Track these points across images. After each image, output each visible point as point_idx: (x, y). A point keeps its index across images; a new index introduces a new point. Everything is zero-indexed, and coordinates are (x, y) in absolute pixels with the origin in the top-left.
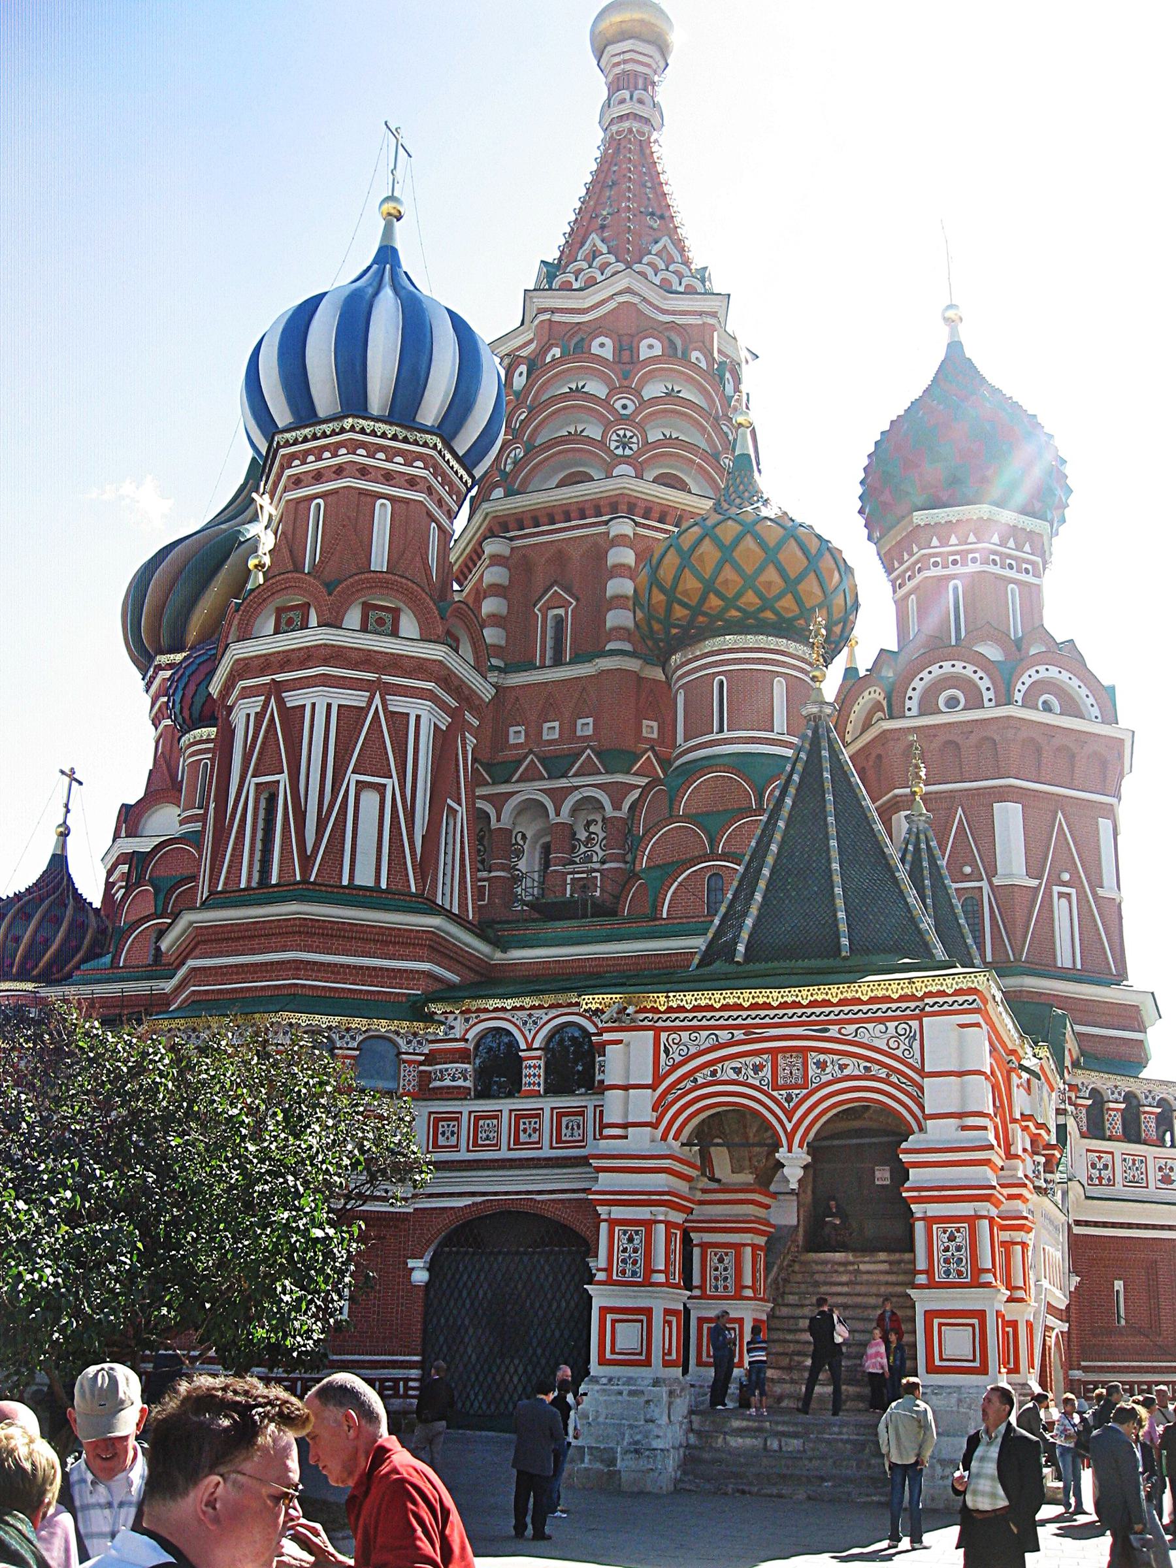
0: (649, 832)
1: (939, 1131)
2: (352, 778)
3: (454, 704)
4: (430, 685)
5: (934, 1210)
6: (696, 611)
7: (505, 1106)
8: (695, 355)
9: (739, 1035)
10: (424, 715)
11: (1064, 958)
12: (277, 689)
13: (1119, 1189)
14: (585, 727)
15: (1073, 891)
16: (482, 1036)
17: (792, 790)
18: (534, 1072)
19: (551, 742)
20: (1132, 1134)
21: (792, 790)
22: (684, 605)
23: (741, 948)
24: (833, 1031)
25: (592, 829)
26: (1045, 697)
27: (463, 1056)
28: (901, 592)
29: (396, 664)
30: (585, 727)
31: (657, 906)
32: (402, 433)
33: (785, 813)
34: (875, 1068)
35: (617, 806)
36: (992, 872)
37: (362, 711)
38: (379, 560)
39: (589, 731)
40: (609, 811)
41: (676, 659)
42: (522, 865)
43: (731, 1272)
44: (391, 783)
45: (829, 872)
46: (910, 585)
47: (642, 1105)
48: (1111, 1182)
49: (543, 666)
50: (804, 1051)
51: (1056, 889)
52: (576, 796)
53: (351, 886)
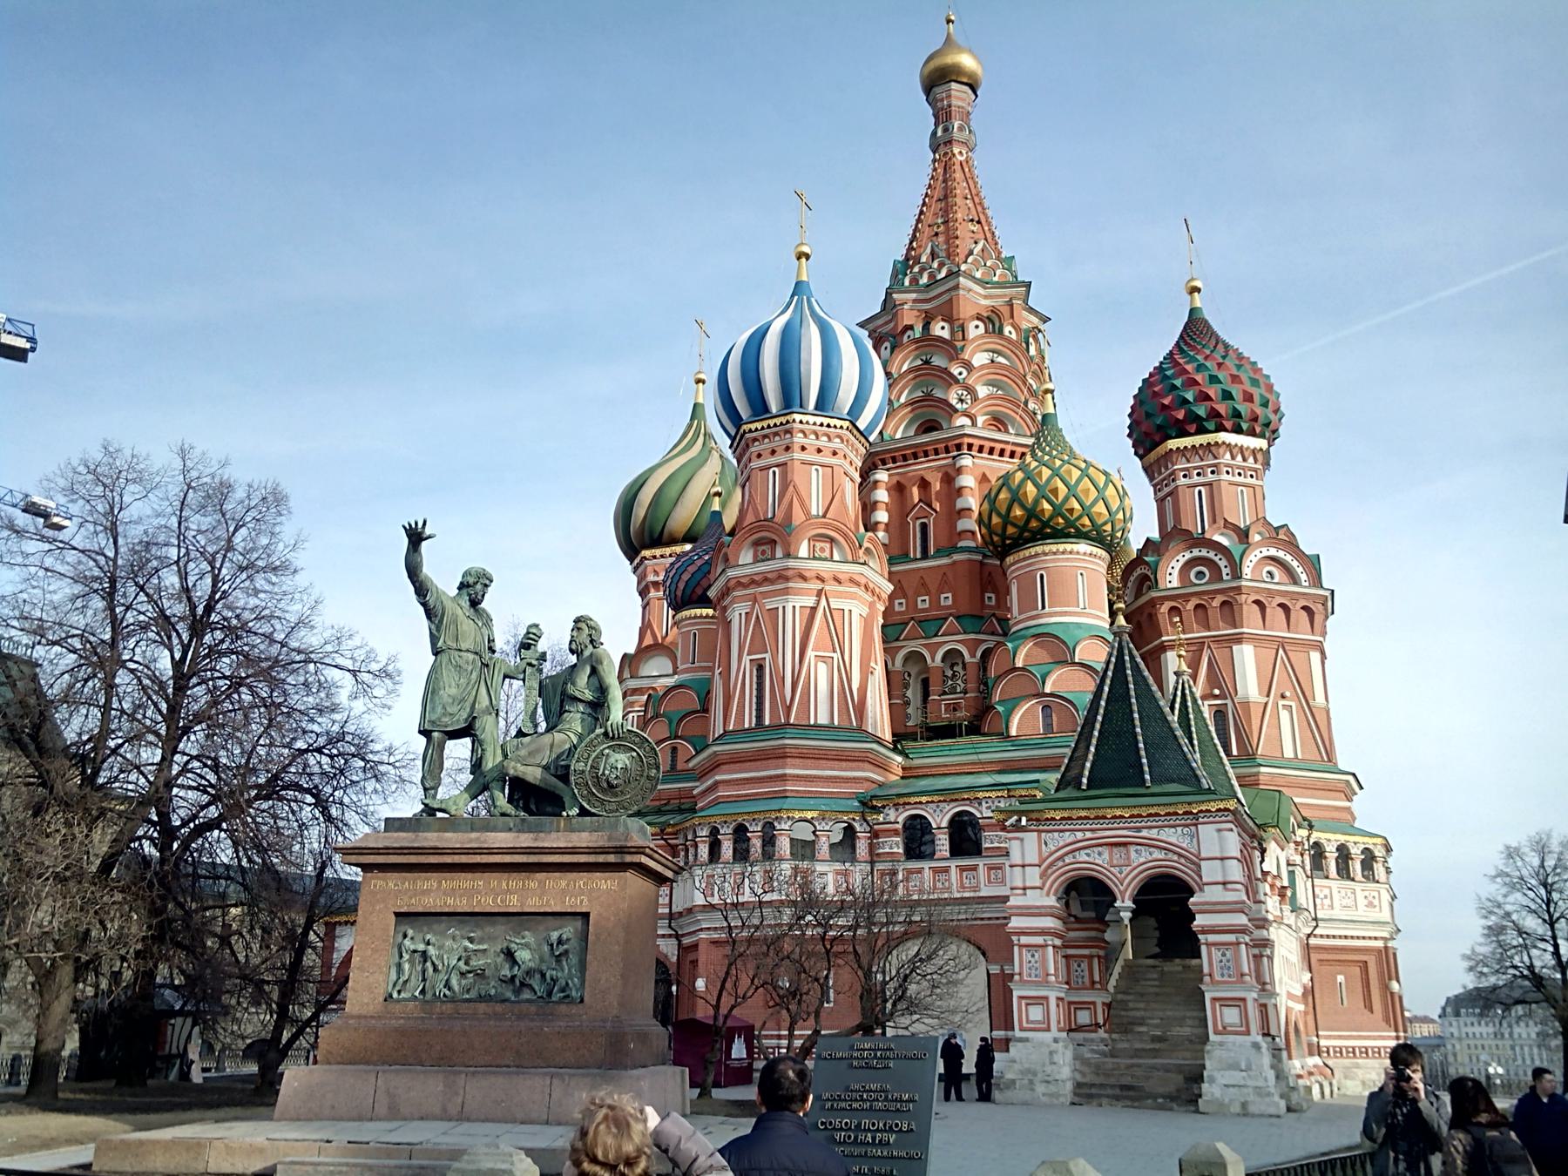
0: (999, 678)
2: (810, 654)
4: (855, 589)
5: (1212, 938)
7: (926, 865)
8: (1007, 329)
9: (1089, 834)
14: (947, 599)
15: (1293, 704)
17: (1108, 681)
19: (924, 610)
20: (1344, 872)
21: (1108, 681)
22: (1014, 525)
23: (1085, 780)
24: (1144, 833)
25: (958, 668)
27: (896, 832)
28: (1160, 495)
30: (947, 599)
32: (826, 421)
33: (1105, 696)
34: (1170, 855)
39: (950, 602)
41: (1010, 560)
42: (909, 693)
43: (1086, 973)
44: (836, 656)
45: (1135, 735)
46: (1166, 490)
47: (1033, 876)
50: (1125, 844)
51: (1281, 702)
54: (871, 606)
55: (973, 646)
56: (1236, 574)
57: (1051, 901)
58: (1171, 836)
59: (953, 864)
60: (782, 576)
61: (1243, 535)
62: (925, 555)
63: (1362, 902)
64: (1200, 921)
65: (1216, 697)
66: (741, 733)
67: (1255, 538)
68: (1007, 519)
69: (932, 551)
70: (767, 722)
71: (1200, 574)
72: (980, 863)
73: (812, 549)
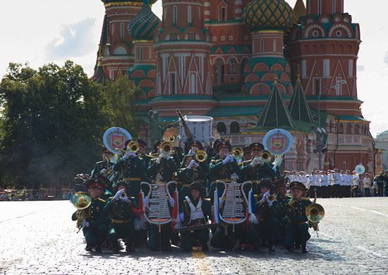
2: (189, 72)
3: (206, 51)
10: (202, 56)
13: (345, 143)
14: (231, 38)
16: (219, 124)
18: (228, 130)
19: (223, 42)
26: (340, 32)
29: (196, 47)
31: (249, 92)
35: (239, 61)
36: (322, 75)
37: (190, 57)
48: (343, 142)
52: (231, 58)
53: (191, 94)
54: (207, 53)
55: (239, 58)
56: (327, 36)
59: (231, 136)
60: (180, 47)
61: (331, 18)
63: (353, 140)
65: (315, 76)
69: (226, 20)
70: (176, 93)
71: (316, 33)
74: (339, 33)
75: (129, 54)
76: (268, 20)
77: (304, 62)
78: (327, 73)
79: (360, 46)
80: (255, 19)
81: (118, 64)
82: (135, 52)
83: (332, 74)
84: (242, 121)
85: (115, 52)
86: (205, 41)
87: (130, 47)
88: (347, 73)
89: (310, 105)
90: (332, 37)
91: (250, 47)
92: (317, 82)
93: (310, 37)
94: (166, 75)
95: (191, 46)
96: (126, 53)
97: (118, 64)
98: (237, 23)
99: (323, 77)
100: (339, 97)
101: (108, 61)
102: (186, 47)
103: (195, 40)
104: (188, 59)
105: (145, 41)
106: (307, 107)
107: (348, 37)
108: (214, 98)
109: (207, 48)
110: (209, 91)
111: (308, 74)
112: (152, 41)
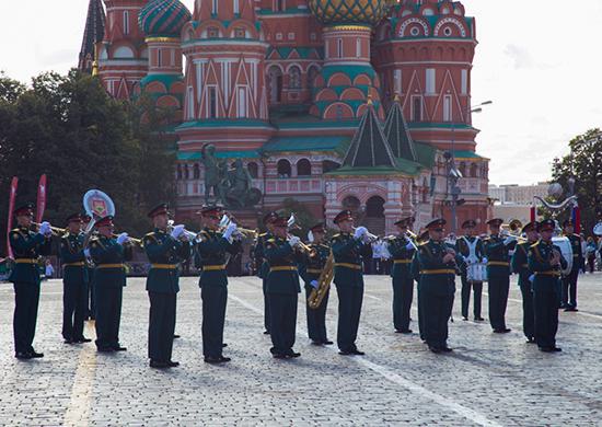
1: (391, 202)
2: (237, 86)
6: (332, 17)
10: (254, 62)
11: (446, 118)
12: (211, 57)
14: (291, 36)
18: (294, 171)
31: (322, 115)
35: (304, 69)
36: (424, 92)
38: (236, 10)
39: (293, 38)
40: (302, 72)
41: (326, 29)
44: (248, 86)
47: (334, 196)
49: (275, 13)
54: (261, 58)
56: (431, 35)
57: (339, 204)
58: (380, 184)
59: (299, 180)
60: (222, 48)
61: (437, 9)
62: (280, 8)
64: (386, 211)
66: (202, 122)
67: (445, 11)
68: (325, 12)
69: (284, 9)
70: (217, 116)
72: (311, 180)
73: (236, 34)
74: (447, 31)
75: (138, 57)
76: (350, 10)
77: (398, 74)
78: (431, 89)
79: (476, 49)
80: (331, 9)
81: (121, 71)
82: (149, 53)
83: (438, 91)
84: (316, 158)
85: (117, 55)
86: (258, 40)
87: (139, 47)
88: (459, 91)
89: (412, 134)
90: (405, 38)
91: (321, 50)
92: (417, 101)
93: (407, 36)
94: (203, 91)
95: (239, 48)
96: (131, 55)
97: (121, 71)
98: (301, 15)
99: (426, 95)
100: (448, 124)
101: (105, 68)
102: (232, 48)
103: (244, 39)
104: (235, 66)
105: (165, 39)
106: (409, 138)
107: (460, 37)
108: (270, 123)
109: (261, 50)
110: (264, 114)
111: (404, 91)
112: (175, 39)
